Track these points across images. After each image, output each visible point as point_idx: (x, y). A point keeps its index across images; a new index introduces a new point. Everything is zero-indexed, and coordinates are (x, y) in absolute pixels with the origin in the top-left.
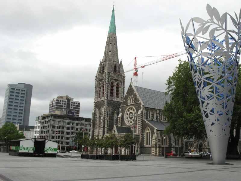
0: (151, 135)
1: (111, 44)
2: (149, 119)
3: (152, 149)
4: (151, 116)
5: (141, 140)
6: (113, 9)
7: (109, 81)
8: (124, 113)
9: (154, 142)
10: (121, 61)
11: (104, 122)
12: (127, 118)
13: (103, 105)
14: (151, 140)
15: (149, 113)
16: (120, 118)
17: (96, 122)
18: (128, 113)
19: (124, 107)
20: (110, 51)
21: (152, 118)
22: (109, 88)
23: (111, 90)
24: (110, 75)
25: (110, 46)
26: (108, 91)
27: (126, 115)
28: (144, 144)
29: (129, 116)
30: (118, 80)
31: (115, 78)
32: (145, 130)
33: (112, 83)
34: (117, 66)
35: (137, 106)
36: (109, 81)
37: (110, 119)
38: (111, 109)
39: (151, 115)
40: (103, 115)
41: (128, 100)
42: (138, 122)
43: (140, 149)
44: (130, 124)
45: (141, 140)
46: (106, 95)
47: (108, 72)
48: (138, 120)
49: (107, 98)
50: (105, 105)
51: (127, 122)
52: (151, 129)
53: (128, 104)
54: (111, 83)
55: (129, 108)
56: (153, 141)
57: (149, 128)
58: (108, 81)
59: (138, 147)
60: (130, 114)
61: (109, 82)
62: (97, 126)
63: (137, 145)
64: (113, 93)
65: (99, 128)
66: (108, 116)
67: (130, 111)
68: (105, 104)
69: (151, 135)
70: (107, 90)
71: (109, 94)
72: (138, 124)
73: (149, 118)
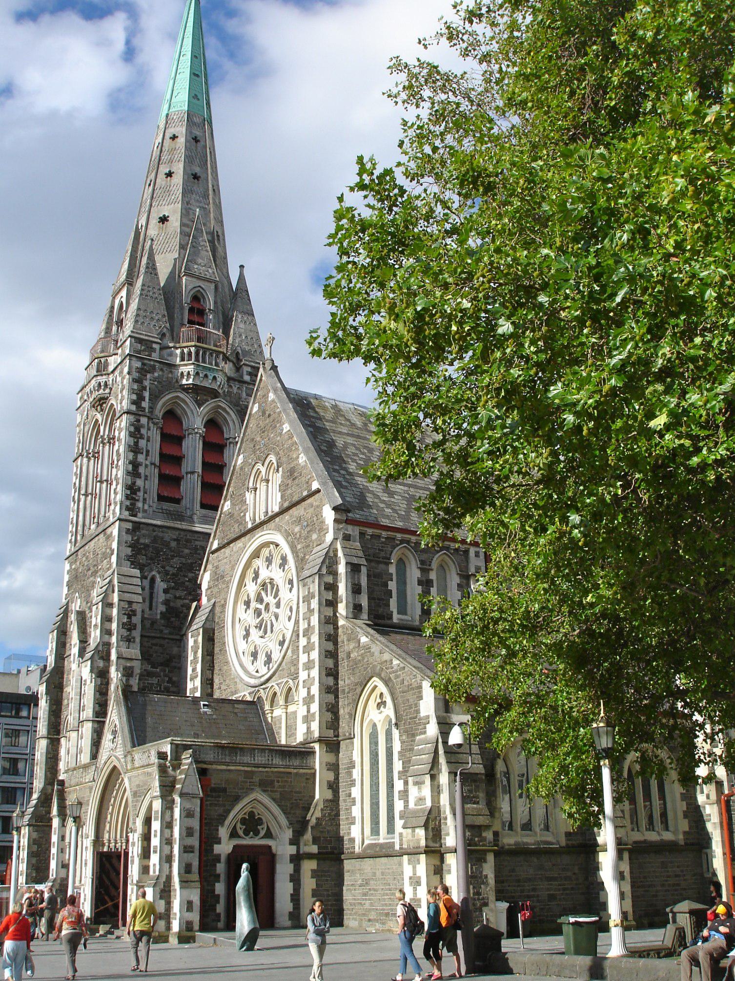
0: (397, 747)
2: (396, 618)
3: (408, 871)
4: (414, 590)
5: (329, 795)
7: (147, 394)
8: (224, 606)
9: (421, 800)
10: (242, 278)
11: (102, 675)
12: (247, 635)
14: (399, 785)
15: (392, 569)
18: (251, 588)
19: (227, 551)
22: (142, 443)
23: (162, 455)
24: (155, 356)
26: (135, 464)
27: (241, 607)
28: (355, 832)
29: (258, 613)
30: (214, 394)
33: (172, 415)
34: (210, 302)
35: (299, 521)
36: (147, 394)
37: (146, 656)
38: (160, 585)
42: (303, 641)
43: (315, 874)
44: (263, 670)
45: (329, 795)
46: (119, 487)
47: (140, 341)
48: (303, 625)
49: (131, 509)
51: (247, 660)
52: (394, 699)
53: (250, 526)
54: (159, 411)
55: (256, 554)
56: (413, 792)
57: (382, 688)
58: (141, 398)
59: (297, 859)
60: (260, 600)
61: (145, 404)
62: (70, 715)
63: (295, 841)
64: (176, 481)
66: (137, 634)
67: (264, 574)
68: (112, 554)
69: (397, 747)
70: (131, 456)
71: (151, 484)
72: (303, 658)
73: (402, 610)
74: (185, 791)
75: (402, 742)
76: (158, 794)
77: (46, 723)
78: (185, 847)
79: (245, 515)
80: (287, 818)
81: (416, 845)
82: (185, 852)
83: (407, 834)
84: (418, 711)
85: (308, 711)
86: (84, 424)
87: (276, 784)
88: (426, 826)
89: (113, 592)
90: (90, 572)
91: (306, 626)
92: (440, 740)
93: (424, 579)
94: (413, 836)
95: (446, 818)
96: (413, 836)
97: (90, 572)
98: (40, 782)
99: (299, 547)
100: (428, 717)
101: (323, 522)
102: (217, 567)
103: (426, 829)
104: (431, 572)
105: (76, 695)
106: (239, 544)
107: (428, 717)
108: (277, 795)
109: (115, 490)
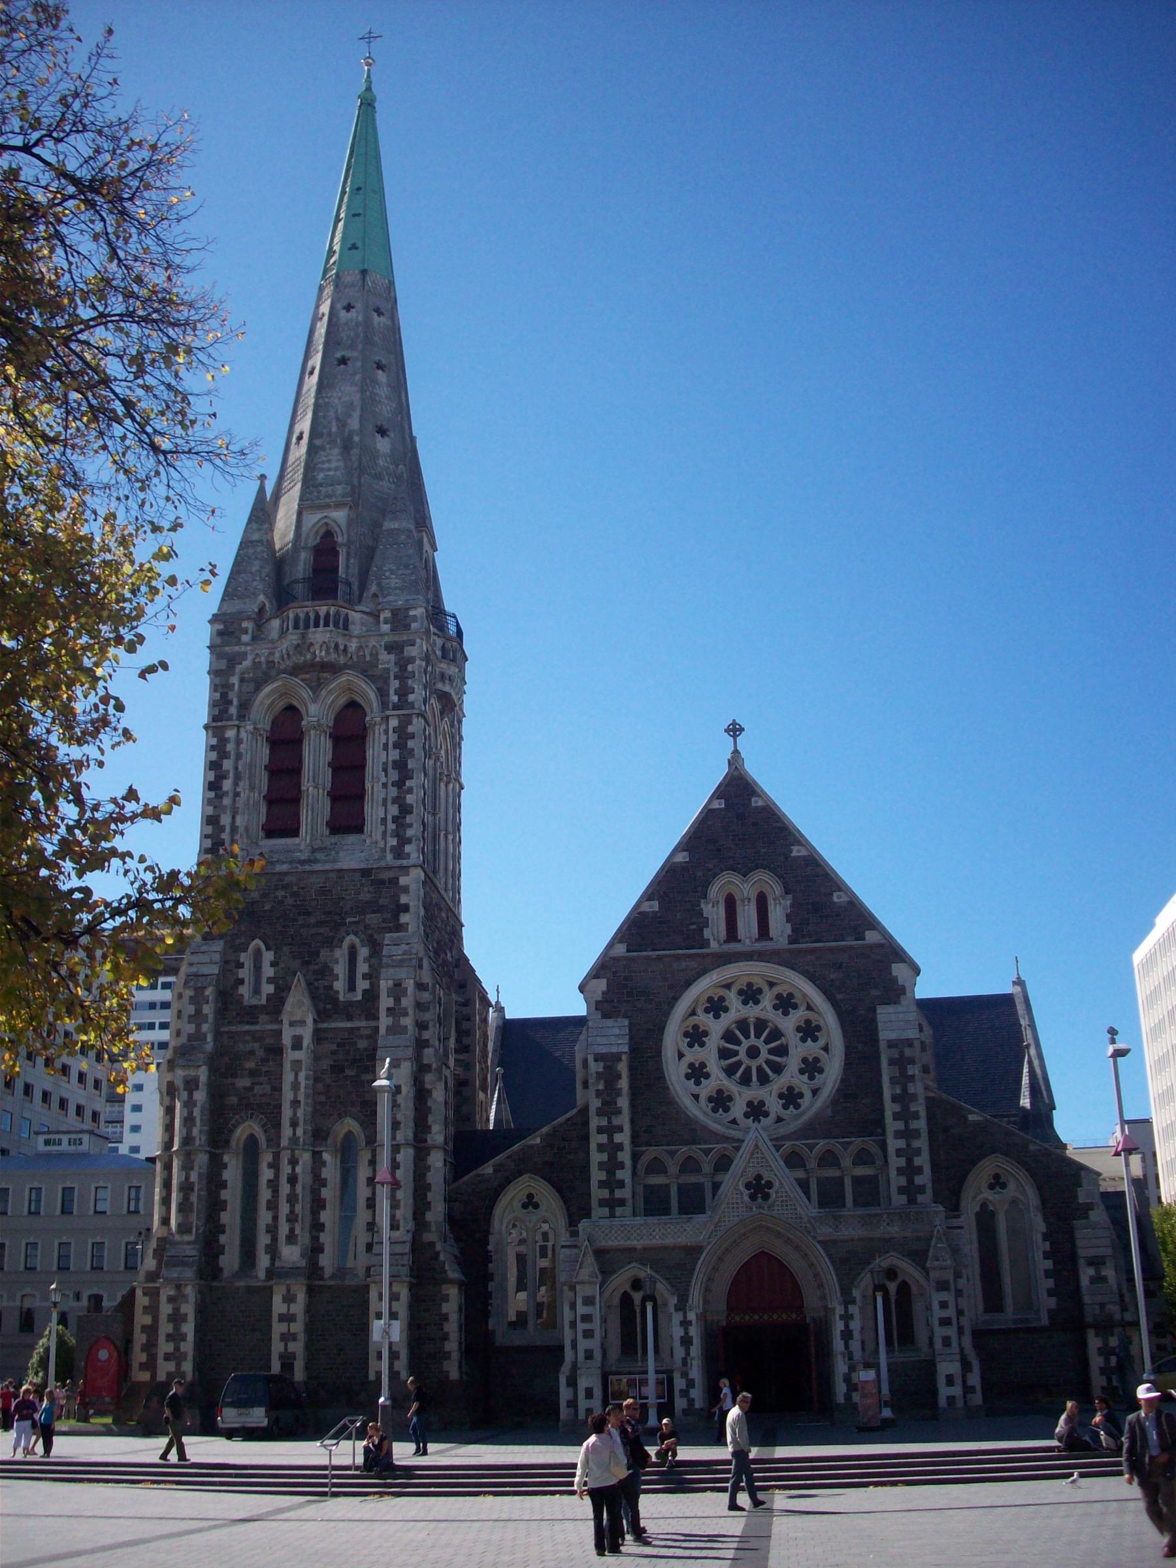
1: (380, 366)
6: (369, 89)
9: (1099, 1279)
13: (372, 919)
16: (623, 1067)
17: (243, 1082)
20: (382, 432)
25: (374, 381)
31: (447, 688)
32: (962, 1180)
35: (839, 966)
40: (407, 1021)
41: (707, 909)
50: (405, 918)
56: (1086, 1273)
65: (316, 1155)
68: (406, 908)
72: (892, 1126)
75: (1048, 1224)
77: (206, 1128)
79: (702, 931)
84: (1076, 1197)
85: (910, 1181)
86: (242, 680)
89: (421, 967)
90: (312, 920)
91: (898, 1091)
97: (312, 920)
98: (198, 1218)
99: (839, 996)
101: (895, 980)
102: (626, 979)
105: (307, 1096)
106: (693, 964)
109: (395, 819)
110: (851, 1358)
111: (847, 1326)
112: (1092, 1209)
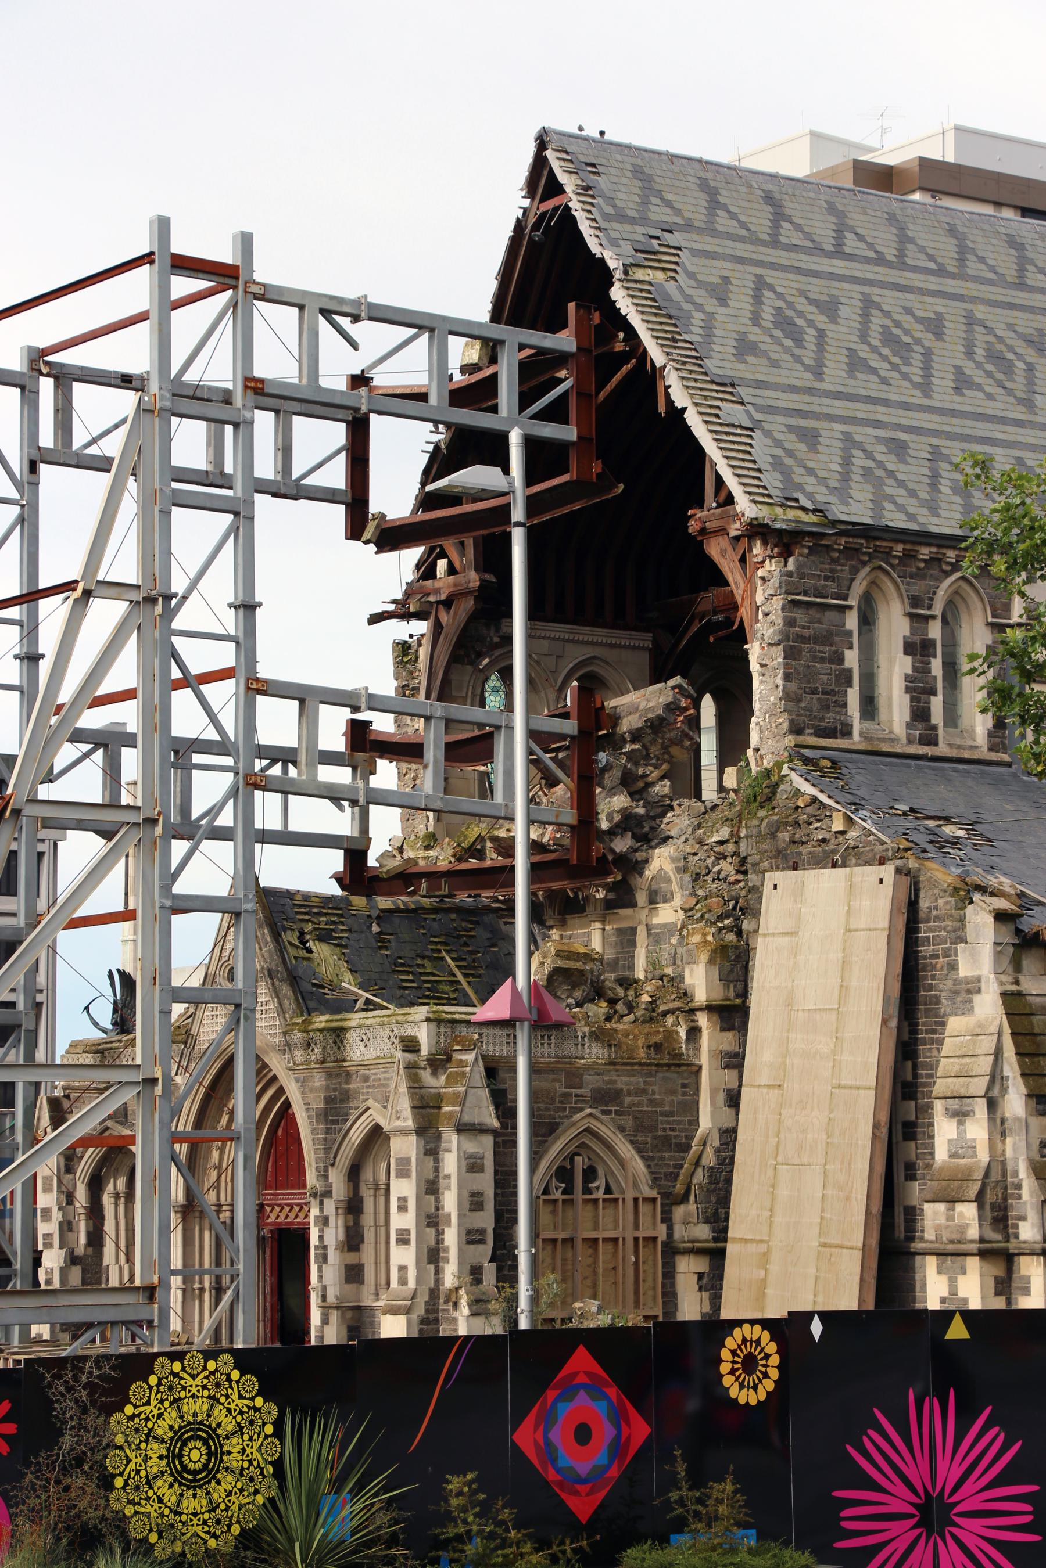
15: (852, 621)
21: (920, 715)
39: (904, 665)
74: (466, 1118)
76: (410, 1123)
78: (469, 1232)
80: (648, 1167)
81: (955, 1236)
82: (470, 1242)
83: (936, 1213)
87: (628, 1100)
88: (980, 1198)
92: (1007, 1030)
93: (917, 639)
94: (951, 1218)
95: (1019, 1186)
96: (951, 1218)
100: (979, 980)
103: (981, 1208)
104: (931, 623)
107: (979, 980)
108: (629, 1122)
110: (324, 1298)
111: (321, 1238)
112: (979, 991)
